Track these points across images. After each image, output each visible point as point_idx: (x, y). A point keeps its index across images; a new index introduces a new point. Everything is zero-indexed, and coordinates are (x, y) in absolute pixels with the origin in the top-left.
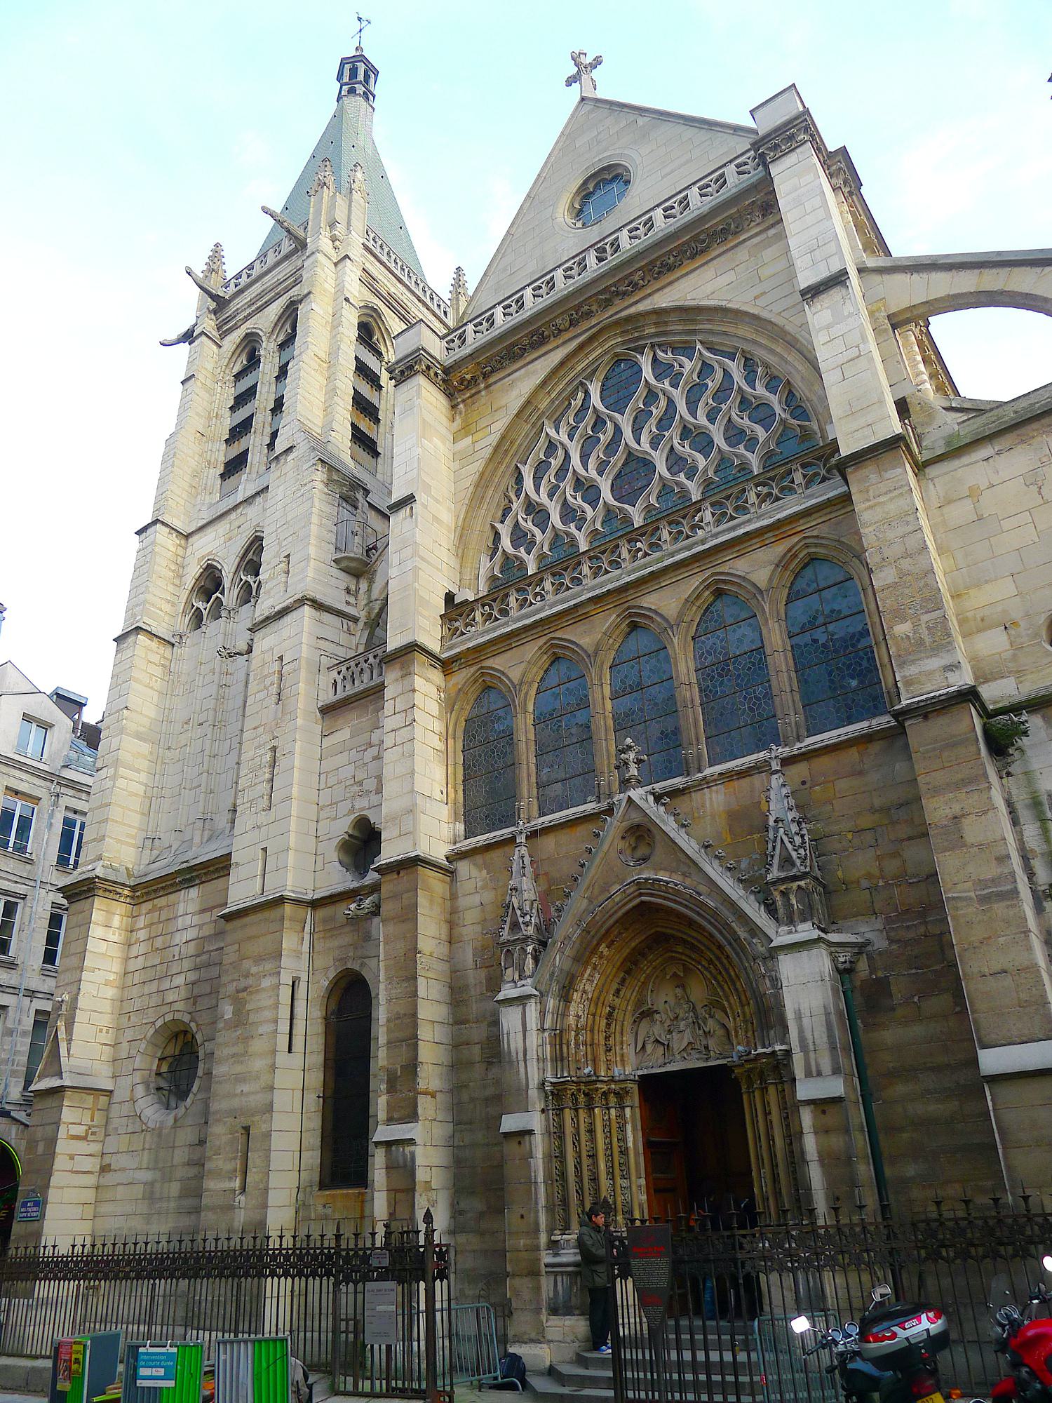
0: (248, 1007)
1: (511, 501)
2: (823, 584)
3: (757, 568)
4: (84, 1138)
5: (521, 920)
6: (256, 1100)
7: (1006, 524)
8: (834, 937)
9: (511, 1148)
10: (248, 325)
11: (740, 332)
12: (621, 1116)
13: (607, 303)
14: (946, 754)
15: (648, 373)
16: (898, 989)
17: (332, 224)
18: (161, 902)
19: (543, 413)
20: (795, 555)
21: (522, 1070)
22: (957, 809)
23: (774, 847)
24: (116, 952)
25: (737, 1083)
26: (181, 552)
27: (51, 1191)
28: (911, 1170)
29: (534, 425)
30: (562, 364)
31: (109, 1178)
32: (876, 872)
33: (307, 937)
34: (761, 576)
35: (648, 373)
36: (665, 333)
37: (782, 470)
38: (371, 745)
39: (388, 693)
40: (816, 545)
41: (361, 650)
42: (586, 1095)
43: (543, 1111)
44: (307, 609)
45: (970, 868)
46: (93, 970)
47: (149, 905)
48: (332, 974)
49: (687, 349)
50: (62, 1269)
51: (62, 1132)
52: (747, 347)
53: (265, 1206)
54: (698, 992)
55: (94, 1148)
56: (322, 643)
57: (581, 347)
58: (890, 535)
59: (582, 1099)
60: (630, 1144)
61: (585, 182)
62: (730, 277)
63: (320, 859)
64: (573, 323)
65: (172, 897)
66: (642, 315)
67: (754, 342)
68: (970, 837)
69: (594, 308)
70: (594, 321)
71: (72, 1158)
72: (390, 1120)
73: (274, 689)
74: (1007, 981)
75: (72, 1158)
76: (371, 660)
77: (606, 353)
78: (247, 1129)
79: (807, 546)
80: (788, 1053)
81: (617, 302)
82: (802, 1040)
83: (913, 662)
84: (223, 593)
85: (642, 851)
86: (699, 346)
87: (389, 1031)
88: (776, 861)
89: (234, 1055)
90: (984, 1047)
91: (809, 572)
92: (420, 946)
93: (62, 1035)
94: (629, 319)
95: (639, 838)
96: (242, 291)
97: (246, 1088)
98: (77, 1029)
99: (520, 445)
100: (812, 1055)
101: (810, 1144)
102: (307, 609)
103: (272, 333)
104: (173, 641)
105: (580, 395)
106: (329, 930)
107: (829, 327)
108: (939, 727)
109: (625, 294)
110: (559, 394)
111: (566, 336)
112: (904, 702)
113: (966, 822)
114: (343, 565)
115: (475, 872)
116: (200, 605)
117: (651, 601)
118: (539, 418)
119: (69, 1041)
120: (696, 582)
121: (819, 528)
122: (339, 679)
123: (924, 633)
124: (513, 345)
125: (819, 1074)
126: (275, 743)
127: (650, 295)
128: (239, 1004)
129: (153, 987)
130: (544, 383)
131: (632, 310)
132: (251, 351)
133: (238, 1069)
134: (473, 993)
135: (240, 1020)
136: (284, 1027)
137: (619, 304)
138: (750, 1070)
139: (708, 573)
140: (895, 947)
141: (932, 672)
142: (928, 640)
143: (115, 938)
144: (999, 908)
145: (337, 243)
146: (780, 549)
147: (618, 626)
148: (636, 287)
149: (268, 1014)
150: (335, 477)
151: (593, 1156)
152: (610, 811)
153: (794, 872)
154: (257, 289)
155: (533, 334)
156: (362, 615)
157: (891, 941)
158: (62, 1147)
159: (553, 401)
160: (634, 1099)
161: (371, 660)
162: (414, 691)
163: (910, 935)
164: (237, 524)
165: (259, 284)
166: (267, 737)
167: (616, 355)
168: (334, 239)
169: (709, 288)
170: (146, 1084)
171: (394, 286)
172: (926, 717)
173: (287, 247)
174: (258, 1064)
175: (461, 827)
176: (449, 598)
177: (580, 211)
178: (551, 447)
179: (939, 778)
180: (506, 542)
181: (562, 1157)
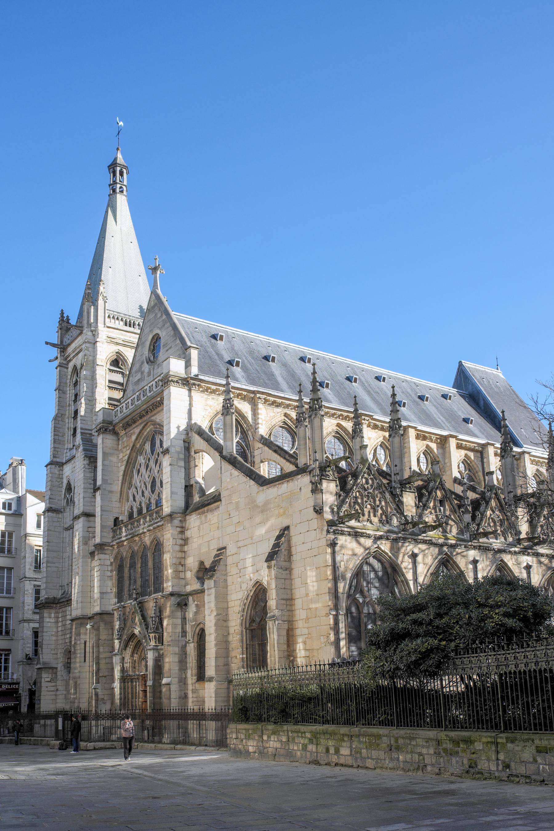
6: (77, 675)
8: (159, 647)
12: (136, 684)
18: (64, 609)
24: (53, 625)
30: (140, 433)
46: (47, 632)
47: (61, 610)
51: (43, 680)
55: (53, 684)
56: (90, 529)
57: (144, 427)
64: (141, 418)
71: (47, 687)
92: (101, 638)
93: (40, 652)
97: (76, 671)
98: (44, 650)
102: (81, 519)
111: (140, 421)
127: (155, 414)
130: (137, 439)
133: (75, 666)
135: (75, 653)
136: (83, 655)
137: (150, 414)
143: (53, 621)
150: (92, 460)
151: (128, 694)
155: (132, 419)
158: (43, 684)
159: (140, 445)
164: (74, 466)
170: (64, 666)
171: (125, 336)
174: (78, 665)
176: (116, 519)
177: (154, 350)
180: (131, 498)
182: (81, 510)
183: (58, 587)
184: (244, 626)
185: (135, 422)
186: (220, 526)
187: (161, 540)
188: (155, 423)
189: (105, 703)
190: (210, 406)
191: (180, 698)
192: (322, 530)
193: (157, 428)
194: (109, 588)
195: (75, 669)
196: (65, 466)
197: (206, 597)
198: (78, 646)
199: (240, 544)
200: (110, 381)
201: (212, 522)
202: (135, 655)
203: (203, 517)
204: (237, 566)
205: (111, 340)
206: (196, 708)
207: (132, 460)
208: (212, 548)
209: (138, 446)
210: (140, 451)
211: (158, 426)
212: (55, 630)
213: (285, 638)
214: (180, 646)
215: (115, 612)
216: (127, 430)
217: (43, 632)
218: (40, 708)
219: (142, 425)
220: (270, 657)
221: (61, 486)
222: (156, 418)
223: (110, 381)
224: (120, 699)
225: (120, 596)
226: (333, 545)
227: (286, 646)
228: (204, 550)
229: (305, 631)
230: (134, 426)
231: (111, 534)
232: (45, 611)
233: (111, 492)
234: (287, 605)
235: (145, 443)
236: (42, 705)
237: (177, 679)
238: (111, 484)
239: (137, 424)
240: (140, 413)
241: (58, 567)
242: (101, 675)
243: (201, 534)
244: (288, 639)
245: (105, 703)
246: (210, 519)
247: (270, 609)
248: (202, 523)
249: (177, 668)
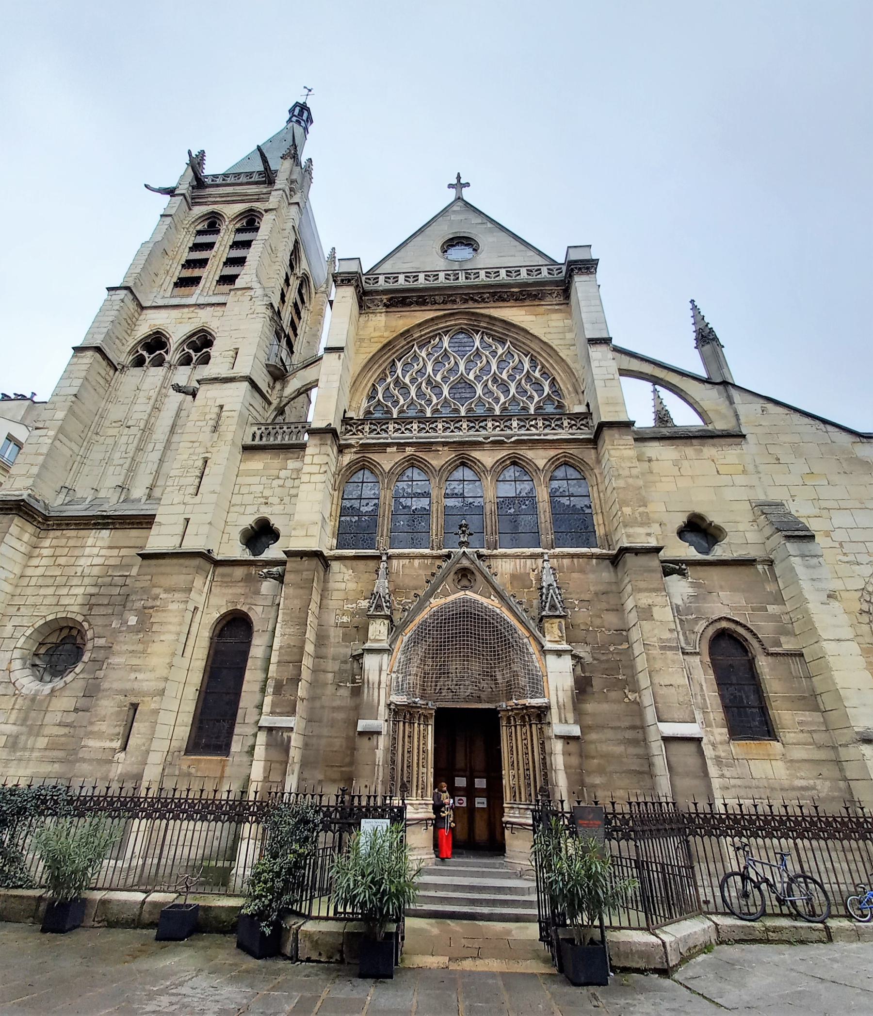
1: (386, 375)
2: (569, 477)
3: (540, 458)
5: (384, 604)
7: (663, 479)
9: (364, 743)
10: (215, 207)
11: (532, 345)
13: (466, 301)
14: (645, 574)
15: (477, 343)
16: (597, 683)
19: (414, 340)
20: (558, 459)
21: (376, 694)
22: (650, 602)
23: (547, 598)
25: (498, 720)
26: (136, 315)
28: (598, 780)
29: (408, 343)
30: (432, 319)
32: (589, 623)
33: (208, 582)
34: (541, 463)
35: (477, 343)
36: (491, 329)
37: (557, 417)
38: (278, 478)
39: (309, 451)
40: (570, 458)
41: (269, 421)
42: (411, 714)
43: (386, 721)
44: (246, 385)
45: (656, 631)
47: (52, 534)
48: (223, 611)
49: (503, 342)
52: (535, 354)
54: (475, 667)
58: (623, 465)
59: (408, 716)
60: (429, 748)
61: (452, 239)
62: (533, 318)
63: (226, 536)
64: (444, 302)
65: (82, 533)
66: (482, 315)
67: (538, 353)
69: (458, 300)
70: (455, 307)
73: (212, 423)
74: (672, 690)
76: (285, 429)
77: (456, 325)
79: (565, 456)
80: (548, 708)
81: (470, 302)
82: (558, 703)
83: (632, 527)
84: (167, 352)
85: (465, 582)
86: (509, 343)
88: (548, 605)
90: (660, 721)
91: (563, 468)
94: (473, 314)
95: (464, 576)
96: (218, 186)
99: (397, 350)
100: (562, 711)
101: (558, 761)
103: (233, 220)
105: (437, 339)
106: (226, 582)
107: (600, 360)
108: (643, 560)
109: (476, 301)
110: (426, 334)
114: (271, 369)
115: (344, 569)
117: (476, 454)
118: (411, 341)
120: (505, 453)
121: (573, 450)
122: (258, 433)
123: (638, 516)
124: (408, 297)
125: (566, 722)
131: (478, 311)
132: (213, 223)
134: (332, 640)
137: (471, 304)
138: (516, 714)
139: (511, 452)
140: (595, 662)
141: (639, 534)
142: (639, 519)
146: (552, 453)
147: (455, 461)
148: (483, 300)
152: (448, 556)
153: (557, 613)
154: (230, 190)
155: (420, 297)
156: (275, 402)
157: (595, 659)
159: (421, 336)
160: (432, 722)
161: (285, 429)
163: (604, 658)
165: (232, 188)
166: (201, 450)
167: (462, 328)
169: (521, 318)
172: (636, 554)
175: (335, 541)
178: (416, 357)
179: (642, 585)
182: (245, 372)
196: (145, 312)
202: (429, 662)
203: (689, 451)
206: (732, 803)
212: (17, 570)
215: (335, 566)
216: (388, 310)
219: (442, 313)
221: (129, 332)
232: (17, 520)
239: (423, 308)
240: (450, 296)
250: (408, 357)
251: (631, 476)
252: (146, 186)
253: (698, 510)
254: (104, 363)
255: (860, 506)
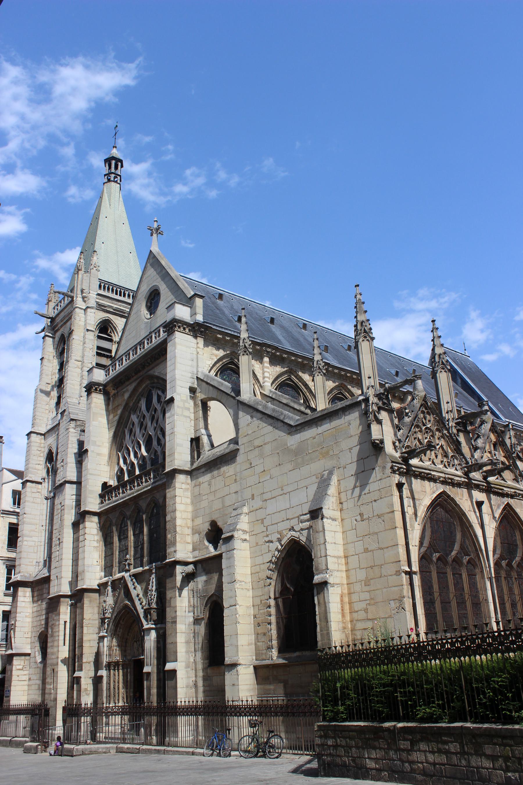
0: (54, 630)
4: (22, 669)
13: (144, 367)
17: (82, 291)
27: (12, 687)
30: (135, 390)
31: (32, 682)
46: (20, 613)
50: (19, 711)
51: (14, 668)
53: (57, 694)
55: (26, 672)
64: (136, 374)
68: (172, 605)
71: (18, 676)
72: (78, 670)
75: (18, 676)
78: (53, 670)
87: (78, 643)
89: (51, 646)
93: (12, 636)
97: (53, 657)
104: (41, 481)
110: (135, 401)
111: (135, 378)
112: (167, 561)
113: (172, 599)
116: (49, 465)
119: (15, 638)
126: (59, 537)
127: (153, 368)
128: (52, 629)
129: (38, 619)
130: (130, 397)
133: (52, 651)
135: (52, 636)
141: (172, 552)
144: (174, 625)
145: (85, 299)
149: (57, 634)
154: (62, 315)
158: (14, 673)
159: (134, 403)
162: (85, 528)
165: (63, 313)
168: (83, 298)
173: (70, 299)
174: (55, 650)
176: (105, 485)
181: (110, 684)
183: (34, 563)
184: (272, 596)
185: (129, 379)
186: (238, 478)
187: (161, 501)
188: (152, 377)
189: (88, 695)
190: (216, 356)
191: (187, 687)
192: (384, 468)
193: (154, 383)
194: (95, 561)
195: (53, 654)
197: (223, 561)
198: (57, 627)
199: (266, 496)
200: (99, 348)
201: (227, 475)
204: (262, 523)
205: (100, 307)
207: (123, 420)
208: (227, 504)
209: (131, 404)
210: (135, 409)
211: (156, 381)
213: (339, 606)
214: (187, 623)
217: (16, 612)
218: (9, 701)
220: (321, 631)
222: (154, 372)
223: (99, 348)
224: (109, 689)
225: (108, 569)
226: (400, 486)
227: (340, 616)
228: (217, 505)
229: (367, 596)
230: (127, 383)
231: (98, 500)
233: (99, 454)
234: (338, 564)
235: (140, 400)
236: (12, 698)
237: (184, 664)
238: (99, 446)
239: (131, 381)
241: (35, 542)
242: (84, 660)
243: (213, 489)
244: (342, 607)
245: (88, 695)
246: (224, 471)
247: (317, 569)
248: (213, 477)
249: (184, 650)
250: (129, 425)
251: (173, 512)
252: (36, 333)
253: (214, 518)
254: (34, 484)
255: (281, 492)
